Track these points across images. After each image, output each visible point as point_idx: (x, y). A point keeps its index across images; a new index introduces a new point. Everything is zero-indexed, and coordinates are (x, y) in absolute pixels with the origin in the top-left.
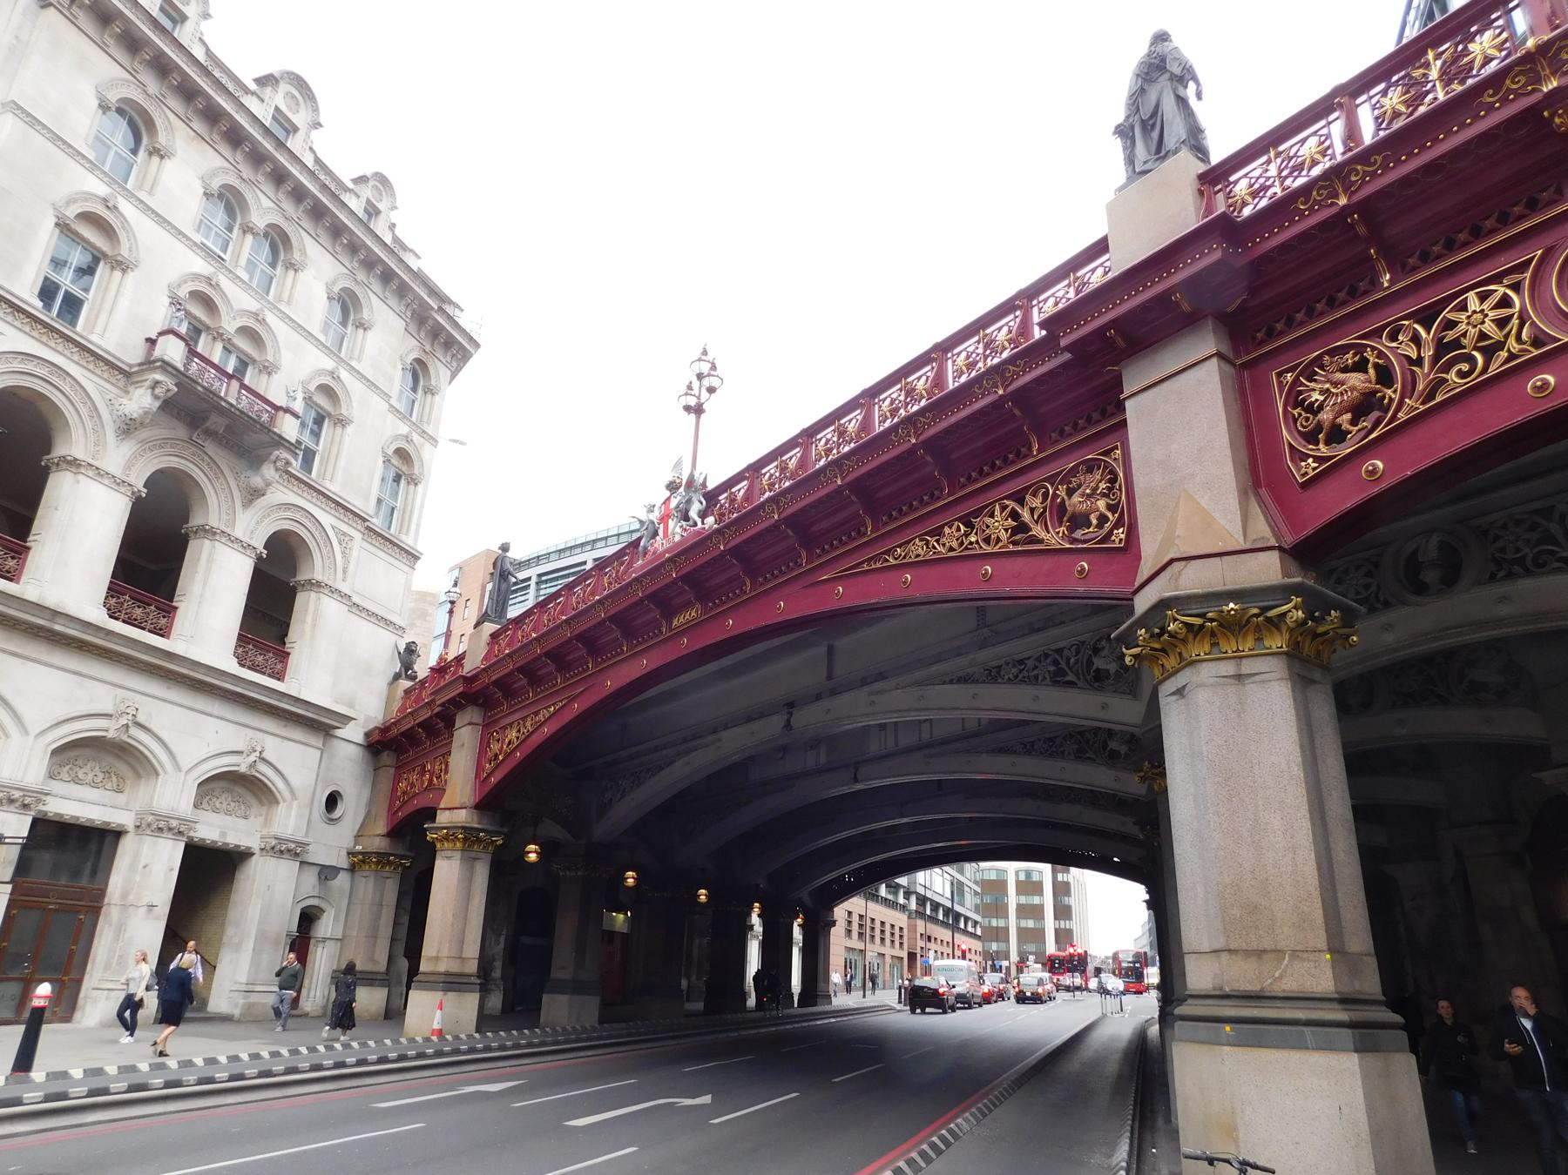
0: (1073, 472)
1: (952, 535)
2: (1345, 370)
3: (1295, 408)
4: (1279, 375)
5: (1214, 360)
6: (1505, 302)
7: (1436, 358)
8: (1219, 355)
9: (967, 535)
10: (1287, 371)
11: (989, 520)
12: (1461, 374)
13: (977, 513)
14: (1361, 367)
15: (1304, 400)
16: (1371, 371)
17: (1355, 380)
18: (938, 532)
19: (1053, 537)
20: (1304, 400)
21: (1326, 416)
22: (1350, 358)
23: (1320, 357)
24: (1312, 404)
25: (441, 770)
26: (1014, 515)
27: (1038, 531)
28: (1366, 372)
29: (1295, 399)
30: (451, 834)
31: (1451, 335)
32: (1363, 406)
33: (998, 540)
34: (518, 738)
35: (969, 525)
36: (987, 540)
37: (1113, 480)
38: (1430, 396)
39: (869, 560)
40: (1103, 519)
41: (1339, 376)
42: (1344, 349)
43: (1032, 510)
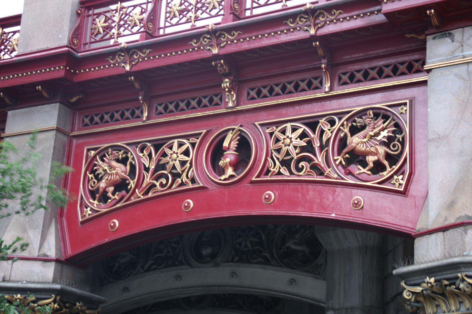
2: (118, 161)
3: (90, 174)
4: (88, 150)
5: (54, 133)
6: (186, 153)
7: (156, 170)
8: (58, 130)
10: (94, 149)
12: (162, 185)
14: (124, 161)
15: (96, 170)
16: (128, 167)
20: (96, 170)
21: (102, 184)
22: (121, 155)
23: (107, 148)
24: (99, 174)
28: (126, 165)
29: (92, 168)
31: (164, 160)
38: (146, 193)
41: (114, 163)
42: (118, 148)
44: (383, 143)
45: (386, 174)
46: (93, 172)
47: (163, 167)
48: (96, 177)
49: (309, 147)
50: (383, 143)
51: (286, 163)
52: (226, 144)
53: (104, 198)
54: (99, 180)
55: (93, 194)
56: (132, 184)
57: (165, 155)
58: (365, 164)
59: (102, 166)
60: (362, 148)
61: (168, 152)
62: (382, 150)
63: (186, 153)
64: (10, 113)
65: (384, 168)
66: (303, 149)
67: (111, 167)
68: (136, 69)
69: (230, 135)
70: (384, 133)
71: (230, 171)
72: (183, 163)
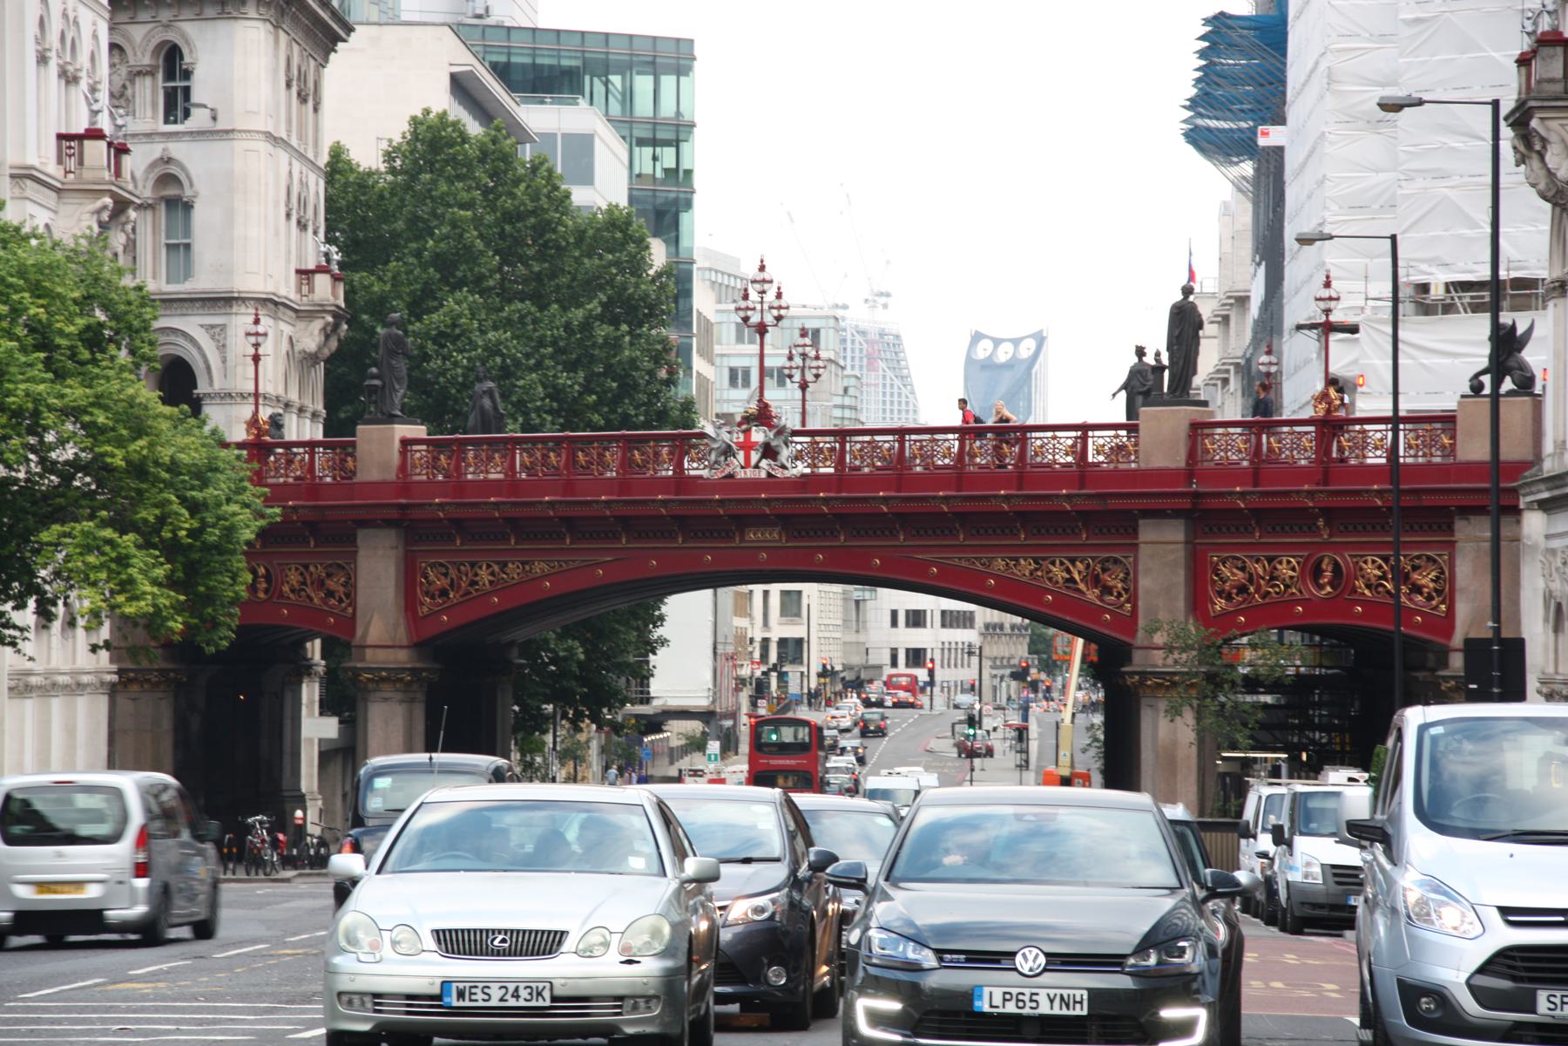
0: (1107, 559)
1: (1026, 567)
9: (1036, 570)
11: (1051, 567)
13: (1044, 559)
14: (1243, 569)
17: (1240, 574)
18: (1017, 559)
19: (1092, 595)
22: (1240, 564)
25: (304, 583)
26: (1068, 571)
27: (1082, 586)
29: (1216, 572)
30: (389, 677)
32: (1242, 589)
33: (1057, 582)
34: (491, 582)
35: (1036, 562)
36: (1050, 579)
37: (1127, 574)
39: (960, 559)
40: (1120, 595)
41: (1235, 571)
43: (1080, 572)
44: (1432, 580)
45: (1434, 603)
46: (1217, 575)
47: (1276, 578)
48: (1221, 579)
49: (1384, 577)
50: (1432, 580)
51: (1368, 586)
52: (1324, 566)
53: (1229, 598)
54: (1224, 582)
55: (1220, 594)
56: (1252, 589)
57: (1275, 568)
58: (1421, 594)
59: (1225, 571)
60: (1419, 582)
61: (1279, 567)
62: (1432, 585)
63: (1293, 569)
64: (1141, 522)
65: (1433, 599)
66: (1380, 578)
67: (1233, 574)
68: (1250, 506)
69: (1326, 560)
70: (1434, 573)
71: (1329, 589)
72: (1291, 577)
